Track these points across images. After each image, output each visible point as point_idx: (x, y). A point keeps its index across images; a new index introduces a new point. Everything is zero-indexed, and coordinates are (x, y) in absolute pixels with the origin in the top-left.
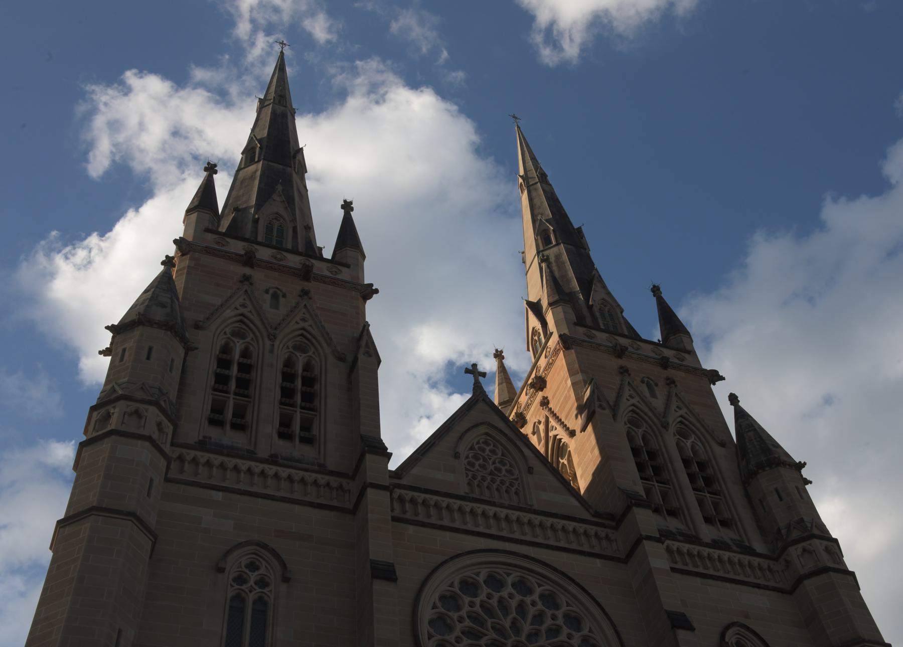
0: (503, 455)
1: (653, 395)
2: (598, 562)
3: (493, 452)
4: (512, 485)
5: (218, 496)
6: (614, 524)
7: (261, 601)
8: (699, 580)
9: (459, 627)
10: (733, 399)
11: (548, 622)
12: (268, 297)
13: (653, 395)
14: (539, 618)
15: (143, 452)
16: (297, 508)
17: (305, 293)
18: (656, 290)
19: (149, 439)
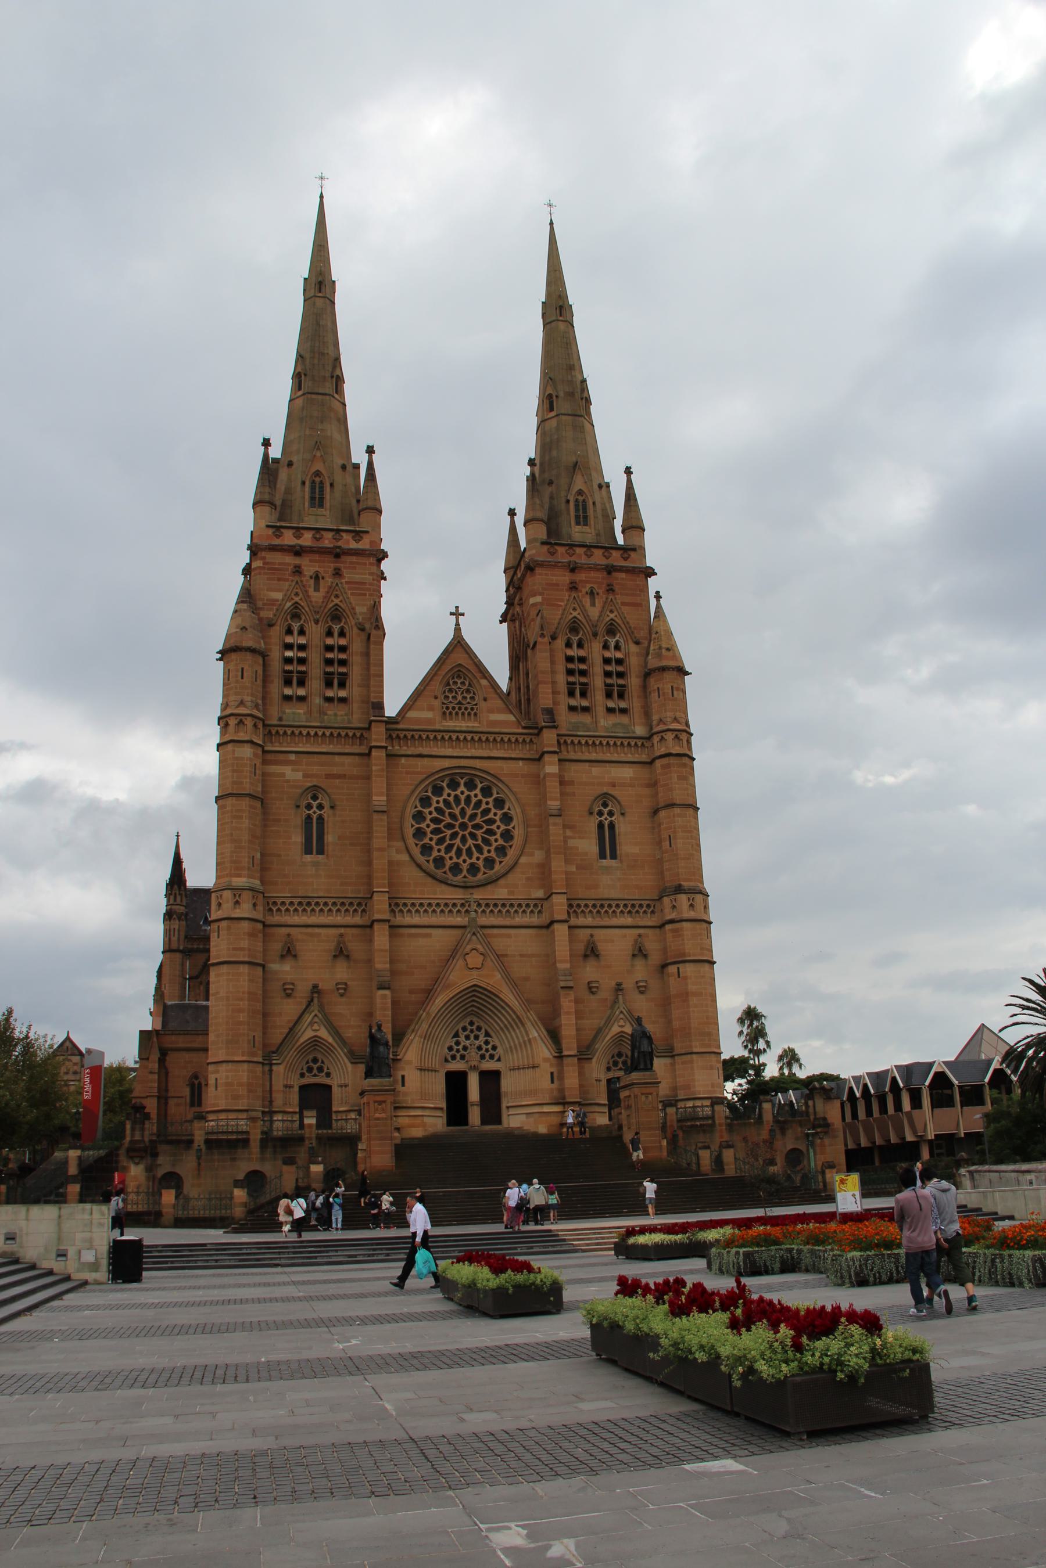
0: (470, 685)
1: (593, 604)
2: (521, 763)
3: (463, 683)
4: (472, 709)
5: (293, 757)
6: (536, 731)
7: (320, 818)
8: (587, 764)
9: (429, 817)
10: (658, 596)
11: (484, 806)
12: (312, 582)
13: (593, 604)
14: (478, 804)
15: (247, 751)
16: (337, 758)
17: (337, 573)
18: (628, 471)
19: (251, 742)
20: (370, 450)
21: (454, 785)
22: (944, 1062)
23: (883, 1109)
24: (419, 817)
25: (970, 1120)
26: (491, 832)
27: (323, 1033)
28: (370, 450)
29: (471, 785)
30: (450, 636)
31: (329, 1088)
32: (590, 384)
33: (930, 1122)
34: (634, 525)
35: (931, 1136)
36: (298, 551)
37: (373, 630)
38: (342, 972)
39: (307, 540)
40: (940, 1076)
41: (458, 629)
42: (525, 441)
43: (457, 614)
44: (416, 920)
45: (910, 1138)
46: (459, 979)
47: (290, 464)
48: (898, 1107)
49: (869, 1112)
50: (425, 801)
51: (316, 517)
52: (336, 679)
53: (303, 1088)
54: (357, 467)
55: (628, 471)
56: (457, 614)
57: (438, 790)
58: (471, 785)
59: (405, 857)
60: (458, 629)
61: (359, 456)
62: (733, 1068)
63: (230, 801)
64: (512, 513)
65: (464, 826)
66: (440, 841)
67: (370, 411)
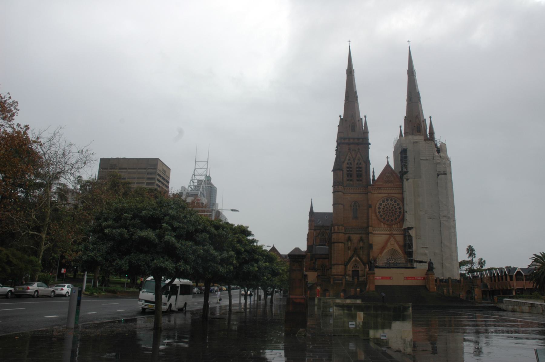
18: (430, 117)
20: (365, 117)
21: (387, 200)
22: (521, 269)
23: (502, 280)
24: (379, 208)
25: (530, 285)
26: (396, 212)
27: (358, 259)
28: (365, 117)
29: (391, 200)
30: (386, 164)
31: (358, 271)
32: (420, 93)
33: (516, 285)
34: (432, 133)
35: (515, 288)
36: (349, 144)
37: (367, 163)
38: (361, 244)
39: (351, 141)
40: (519, 273)
41: (388, 162)
42: (403, 112)
43: (388, 158)
44: (379, 232)
45: (509, 288)
46: (389, 247)
47: (346, 121)
48: (506, 280)
49: (499, 281)
50: (381, 204)
51: (352, 137)
52: (359, 175)
53: (352, 271)
54: (362, 119)
55: (430, 117)
56: (388, 158)
57: (384, 201)
58: (391, 200)
59: (375, 218)
60: (388, 162)
61: (362, 116)
62: (463, 263)
63: (336, 205)
64: (401, 127)
65: (390, 210)
66: (384, 214)
67: (365, 109)
